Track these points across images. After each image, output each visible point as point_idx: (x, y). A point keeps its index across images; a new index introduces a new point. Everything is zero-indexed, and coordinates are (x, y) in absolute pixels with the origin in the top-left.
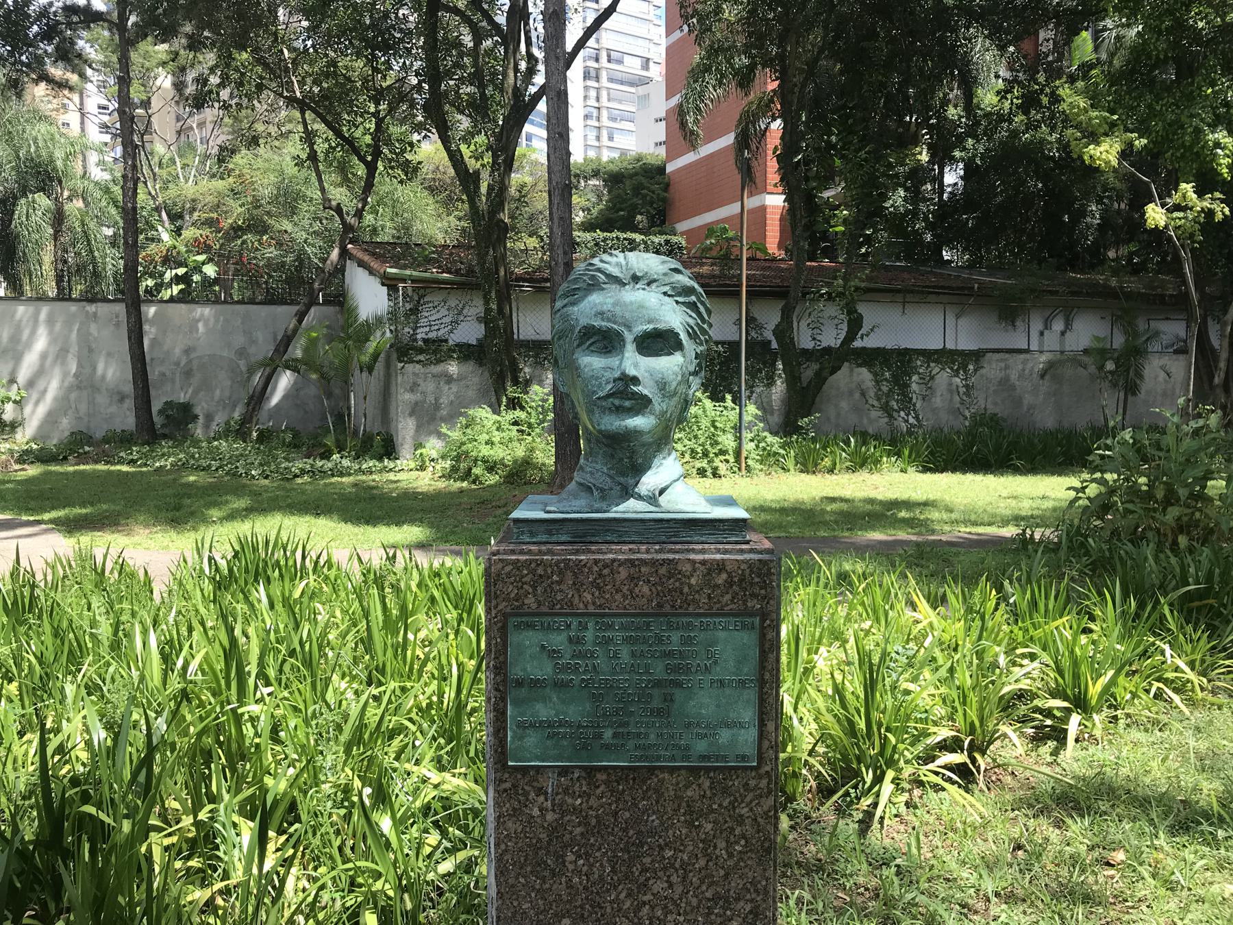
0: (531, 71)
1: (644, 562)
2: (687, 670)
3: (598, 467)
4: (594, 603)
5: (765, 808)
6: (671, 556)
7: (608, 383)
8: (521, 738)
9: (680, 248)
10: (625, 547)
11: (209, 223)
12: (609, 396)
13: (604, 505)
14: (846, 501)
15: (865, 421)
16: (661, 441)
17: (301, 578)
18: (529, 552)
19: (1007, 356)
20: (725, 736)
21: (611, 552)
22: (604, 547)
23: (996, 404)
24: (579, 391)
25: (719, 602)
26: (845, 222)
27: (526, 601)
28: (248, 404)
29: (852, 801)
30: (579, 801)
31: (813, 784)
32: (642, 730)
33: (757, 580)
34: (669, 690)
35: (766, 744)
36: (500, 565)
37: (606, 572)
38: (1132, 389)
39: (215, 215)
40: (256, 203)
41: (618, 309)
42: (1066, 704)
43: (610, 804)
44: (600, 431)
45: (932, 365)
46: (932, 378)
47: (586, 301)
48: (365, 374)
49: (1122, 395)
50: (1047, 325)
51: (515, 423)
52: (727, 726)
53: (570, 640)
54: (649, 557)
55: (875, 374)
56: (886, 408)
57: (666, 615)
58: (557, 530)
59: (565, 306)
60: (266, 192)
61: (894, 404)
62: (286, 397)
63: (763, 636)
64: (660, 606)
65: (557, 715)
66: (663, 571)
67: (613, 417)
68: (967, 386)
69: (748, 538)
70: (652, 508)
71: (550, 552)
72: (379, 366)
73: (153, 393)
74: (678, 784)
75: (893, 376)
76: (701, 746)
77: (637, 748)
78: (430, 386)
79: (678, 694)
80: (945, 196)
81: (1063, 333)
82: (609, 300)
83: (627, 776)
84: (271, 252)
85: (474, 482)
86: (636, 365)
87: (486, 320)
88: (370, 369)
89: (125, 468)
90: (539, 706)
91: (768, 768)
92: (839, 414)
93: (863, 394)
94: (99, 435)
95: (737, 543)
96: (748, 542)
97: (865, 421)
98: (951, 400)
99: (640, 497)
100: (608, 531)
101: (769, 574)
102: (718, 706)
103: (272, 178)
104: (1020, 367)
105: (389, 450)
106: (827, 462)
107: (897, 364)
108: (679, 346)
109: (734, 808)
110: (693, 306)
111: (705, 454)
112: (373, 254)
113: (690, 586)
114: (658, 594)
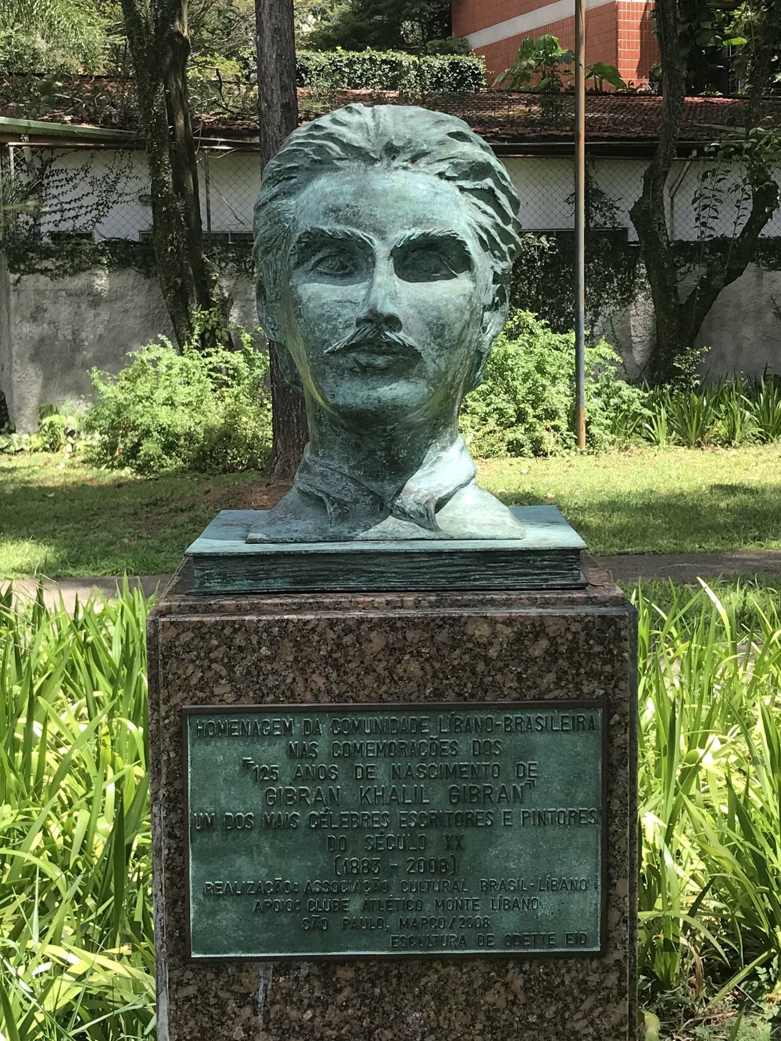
2: (485, 797)
3: (334, 464)
4: (329, 692)
5: (614, 1019)
6: (455, 612)
7: (348, 327)
8: (213, 913)
9: (476, 77)
10: (380, 599)
12: (349, 348)
13: (343, 529)
16: (439, 422)
18: (221, 610)
20: (546, 904)
21: (356, 606)
22: (344, 599)
24: (300, 340)
27: (217, 691)
29: (761, 987)
30: (309, 1014)
31: (698, 960)
32: (411, 897)
33: (597, 649)
34: (455, 831)
35: (615, 916)
36: (172, 632)
37: (348, 639)
41: (363, 203)
43: (360, 1019)
44: (336, 407)
47: (310, 188)
52: (551, 888)
53: (291, 752)
54: (418, 613)
57: (447, 709)
59: (274, 197)
63: (608, 740)
64: (438, 694)
65: (270, 875)
66: (442, 636)
69: (582, 580)
70: (424, 533)
71: (256, 609)
74: (470, 983)
76: (509, 922)
77: (403, 925)
78: (63, 312)
79: (470, 836)
82: (347, 188)
83: (388, 971)
86: (394, 297)
87: (154, 199)
90: (241, 862)
91: (618, 955)
92: (739, 350)
95: (564, 588)
96: (582, 587)
99: (404, 515)
100: (350, 571)
102: (536, 856)
106: (721, 428)
108: (465, 263)
109: (564, 1021)
110: (488, 196)
111: (521, 417)
113: (487, 660)
114: (435, 675)
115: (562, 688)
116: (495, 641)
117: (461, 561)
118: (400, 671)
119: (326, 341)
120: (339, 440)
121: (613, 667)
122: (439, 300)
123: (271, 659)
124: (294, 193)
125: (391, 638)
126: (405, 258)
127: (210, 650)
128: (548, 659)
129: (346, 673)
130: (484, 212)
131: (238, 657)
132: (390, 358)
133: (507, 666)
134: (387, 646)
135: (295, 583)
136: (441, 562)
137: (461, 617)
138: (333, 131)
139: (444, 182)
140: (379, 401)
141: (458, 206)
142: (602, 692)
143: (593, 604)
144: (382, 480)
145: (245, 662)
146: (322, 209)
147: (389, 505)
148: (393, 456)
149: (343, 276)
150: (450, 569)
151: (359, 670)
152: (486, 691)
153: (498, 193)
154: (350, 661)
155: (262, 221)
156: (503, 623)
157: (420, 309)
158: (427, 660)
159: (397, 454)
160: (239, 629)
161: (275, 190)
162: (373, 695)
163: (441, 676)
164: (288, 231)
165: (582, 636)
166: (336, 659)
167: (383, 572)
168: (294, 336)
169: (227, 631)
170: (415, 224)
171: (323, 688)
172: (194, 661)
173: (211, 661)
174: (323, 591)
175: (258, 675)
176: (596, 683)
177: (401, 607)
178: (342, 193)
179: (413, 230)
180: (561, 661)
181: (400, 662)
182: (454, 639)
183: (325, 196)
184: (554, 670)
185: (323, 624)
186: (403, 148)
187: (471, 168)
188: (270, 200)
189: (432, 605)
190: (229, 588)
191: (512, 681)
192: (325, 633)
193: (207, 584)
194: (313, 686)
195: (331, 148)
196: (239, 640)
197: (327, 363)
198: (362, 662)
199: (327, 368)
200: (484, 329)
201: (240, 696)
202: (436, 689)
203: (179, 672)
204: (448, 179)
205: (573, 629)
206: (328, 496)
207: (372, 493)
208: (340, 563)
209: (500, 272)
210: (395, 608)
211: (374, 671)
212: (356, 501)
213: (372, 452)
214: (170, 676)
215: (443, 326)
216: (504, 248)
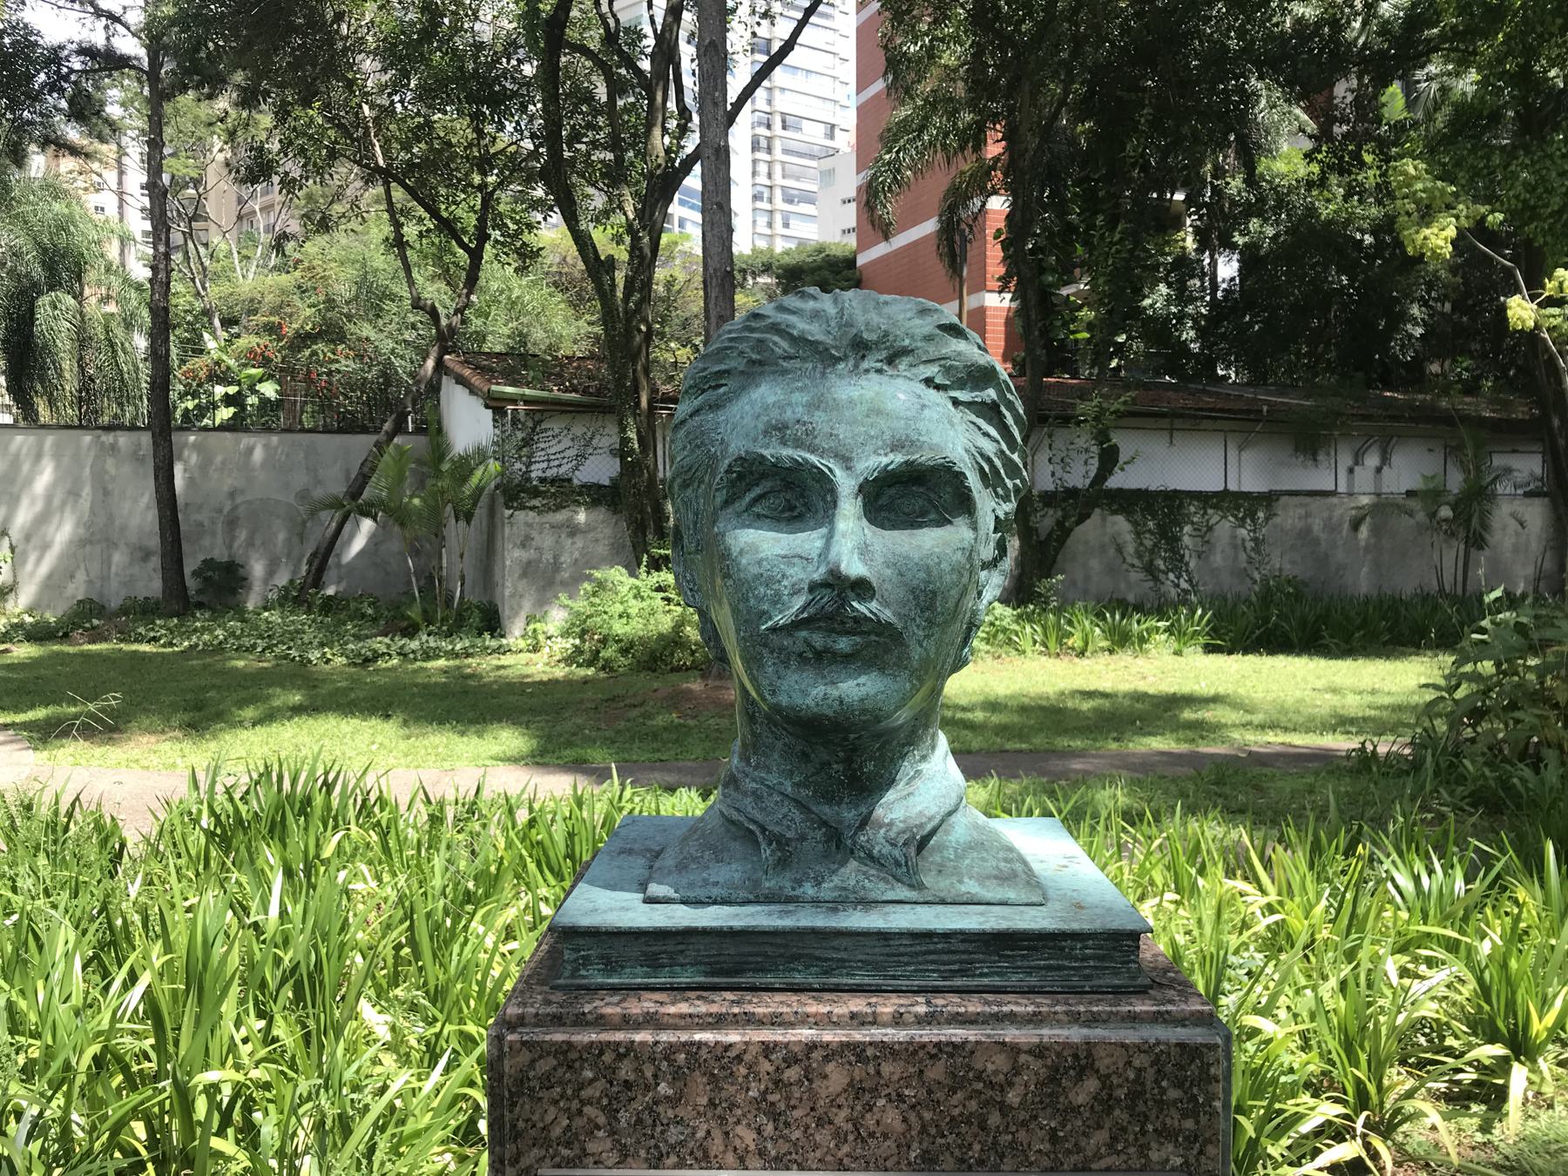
0: (683, 130)
1: (887, 1050)
7: (795, 592)
11: (272, 329)
12: (797, 625)
15: (1123, 586)
17: (336, 827)
19: (1308, 500)
21: (803, 1020)
23: (1293, 563)
25: (1078, 1149)
26: (1090, 327)
27: (592, 1147)
28: (310, 563)
33: (1173, 1094)
36: (525, 1057)
37: (793, 1074)
38: (1477, 541)
39: (275, 319)
40: (330, 302)
41: (819, 418)
42: (1499, 1050)
44: (777, 709)
45: (1210, 511)
46: (1210, 529)
47: (744, 400)
48: (462, 523)
49: (1462, 546)
50: (1358, 460)
51: (659, 589)
54: (901, 1035)
55: (1135, 524)
56: (1150, 569)
58: (671, 956)
60: (343, 289)
61: (1160, 564)
62: (361, 553)
66: (936, 1072)
67: (808, 675)
68: (1255, 540)
72: (480, 513)
73: (185, 547)
75: (1158, 525)
78: (547, 541)
80: (1219, 294)
81: (1379, 470)
82: (798, 397)
84: (347, 365)
85: (603, 668)
87: (622, 452)
88: (468, 520)
89: (145, 648)
92: (1087, 578)
93: (1120, 549)
94: (114, 604)
96: (1142, 991)
97: (1123, 586)
98: (1236, 558)
100: (796, 958)
101: (1206, 1078)
103: (352, 272)
104: (1326, 514)
105: (492, 623)
106: (1076, 641)
107: (1163, 510)
110: (990, 412)
112: (477, 367)
113: (1004, 1109)
114: (924, 1130)
115: (1118, 1153)
116: (1017, 1080)
117: (962, 947)
118: (870, 1121)
120: (779, 744)
121: (1197, 1122)
122: (928, 556)
123: (674, 1101)
125: (858, 1072)
126: (878, 496)
127: (581, 1087)
129: (787, 1125)
130: (986, 434)
132: (858, 639)
133: (1035, 1117)
134: (851, 1084)
135: (713, 974)
136: (932, 947)
137: (965, 1042)
139: (932, 392)
142: (1179, 1161)
144: (839, 804)
145: (635, 1105)
146: (761, 427)
147: (849, 842)
150: (945, 957)
151: (808, 1120)
152: (1002, 1156)
153: (1003, 409)
154: (794, 1107)
155: (679, 444)
156: (1030, 1052)
157: (900, 567)
158: (913, 1107)
159: (861, 767)
161: (696, 403)
163: (933, 1131)
164: (714, 457)
165: (1150, 1074)
166: (773, 1104)
167: (843, 960)
168: (720, 603)
169: (608, 1057)
170: (894, 448)
171: (752, 1147)
172: (556, 1102)
173: (582, 1103)
174: (754, 989)
176: (1170, 1148)
177: (873, 1023)
179: (891, 456)
180: (1117, 1112)
181: (871, 1110)
182: (954, 1076)
183: (766, 408)
184: (1107, 1126)
185: (753, 1050)
189: (921, 1021)
192: (756, 1064)
194: (738, 1142)
195: (775, 343)
196: (625, 1071)
197: (766, 644)
198: (812, 1109)
199: (765, 652)
200: (980, 594)
202: (925, 1152)
203: (535, 1118)
204: (938, 387)
205: (1137, 1063)
206: (763, 829)
207: (825, 824)
208: (779, 946)
209: (1002, 516)
210: (863, 1024)
211: (831, 1122)
212: (802, 838)
213: (826, 765)
214: (521, 1124)
215: (934, 593)
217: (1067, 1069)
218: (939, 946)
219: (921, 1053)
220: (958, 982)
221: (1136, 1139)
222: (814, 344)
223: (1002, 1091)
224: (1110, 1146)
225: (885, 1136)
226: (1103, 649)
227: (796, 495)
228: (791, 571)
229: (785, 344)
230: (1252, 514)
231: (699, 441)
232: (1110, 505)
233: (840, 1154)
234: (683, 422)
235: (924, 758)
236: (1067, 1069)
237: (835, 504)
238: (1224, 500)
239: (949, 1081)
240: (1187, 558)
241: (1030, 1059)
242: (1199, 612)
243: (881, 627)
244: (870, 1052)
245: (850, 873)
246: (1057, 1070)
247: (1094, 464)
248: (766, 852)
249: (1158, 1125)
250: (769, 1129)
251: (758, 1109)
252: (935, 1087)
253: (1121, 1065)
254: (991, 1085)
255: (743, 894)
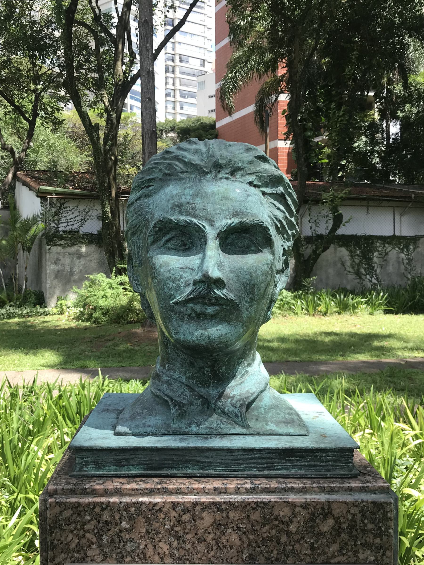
7: (187, 285)
13: (182, 425)
14: (336, 334)
15: (345, 281)
18: (94, 493)
21: (192, 491)
25: (324, 553)
26: (328, 157)
37: (186, 517)
41: (198, 202)
44: (178, 341)
46: (387, 254)
51: (121, 284)
54: (238, 498)
55: (351, 252)
56: (358, 274)
58: (128, 461)
61: (363, 271)
66: (256, 516)
67: (193, 325)
68: (408, 259)
75: (362, 252)
80: (391, 141)
92: (328, 278)
93: (343, 264)
97: (345, 281)
98: (399, 268)
106: (322, 308)
107: (364, 245)
110: (281, 198)
113: (288, 534)
114: (250, 544)
115: (344, 555)
116: (294, 520)
118: (224, 540)
119: (172, 295)
120: (179, 359)
122: (250, 268)
124: (152, 196)
125: (218, 516)
126: (226, 239)
128: (333, 533)
129: (184, 542)
130: (279, 209)
131: (105, 529)
132: (217, 308)
133: (304, 538)
134: (214, 522)
135: (148, 469)
136: (253, 456)
137: (270, 502)
138: (178, 154)
139: (252, 188)
140: (209, 338)
141: (262, 204)
143: (366, 491)
144: (208, 387)
146: (170, 205)
148: (216, 371)
149: (184, 250)
150: (260, 461)
151: (194, 539)
152: (288, 557)
153: (287, 196)
154: (187, 533)
155: (130, 214)
157: (237, 273)
158: (244, 533)
159: (219, 370)
160: (106, 509)
161: (139, 194)
162: (204, 558)
163: (254, 545)
164: (147, 220)
166: (177, 532)
167: (210, 462)
168: (151, 291)
170: (235, 215)
174: (168, 476)
175: (120, 542)
177: (225, 493)
178: (184, 195)
179: (233, 220)
181: (224, 534)
182: (264, 518)
183: (172, 197)
186: (225, 165)
187: (270, 180)
188: (136, 200)
190: (100, 473)
191: (307, 549)
193: (85, 469)
195: (177, 165)
198: (196, 534)
199: (172, 314)
200: (276, 285)
201: (106, 557)
204: (255, 186)
205: (352, 511)
206: (172, 399)
207: (201, 397)
208: (180, 455)
209: (286, 248)
211: (205, 541)
212: (191, 404)
215: (254, 285)
216: (290, 232)
217: (318, 515)
218: (257, 455)
219: (248, 507)
220: (266, 473)
221: (352, 548)
222: (195, 166)
223: (287, 525)
224: (340, 551)
225: (231, 547)
226: (335, 312)
227: (188, 239)
228: (184, 275)
229: (181, 166)
230: (407, 247)
231: (140, 212)
232: (338, 243)
233: (209, 556)
234: (132, 203)
235: (249, 365)
236: (318, 515)
237: (206, 242)
238: (394, 240)
239: (261, 521)
240: (375, 268)
241: (301, 509)
242: (382, 294)
243: (228, 302)
244: (223, 507)
245: (214, 420)
246: (314, 515)
247: (331, 223)
248: (173, 410)
249: (363, 541)
250: (175, 544)
251: (170, 534)
252: (255, 524)
253: (345, 512)
254: (282, 522)
255: (162, 431)
